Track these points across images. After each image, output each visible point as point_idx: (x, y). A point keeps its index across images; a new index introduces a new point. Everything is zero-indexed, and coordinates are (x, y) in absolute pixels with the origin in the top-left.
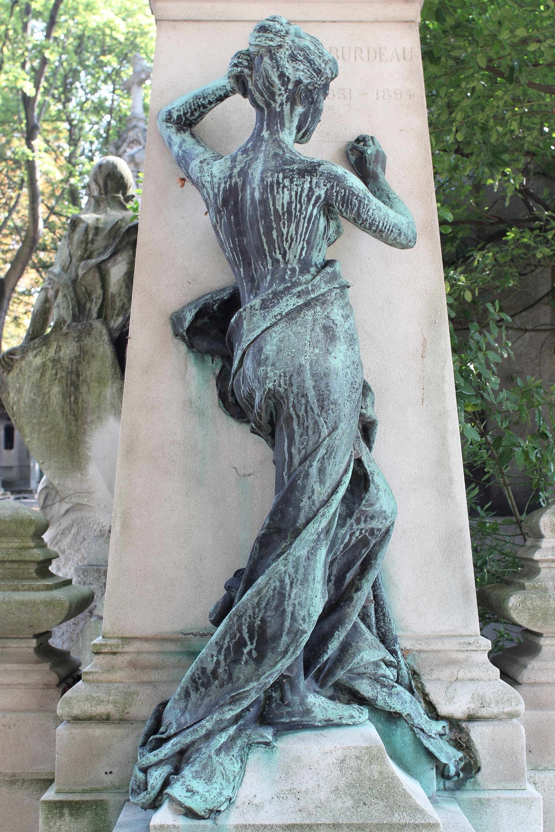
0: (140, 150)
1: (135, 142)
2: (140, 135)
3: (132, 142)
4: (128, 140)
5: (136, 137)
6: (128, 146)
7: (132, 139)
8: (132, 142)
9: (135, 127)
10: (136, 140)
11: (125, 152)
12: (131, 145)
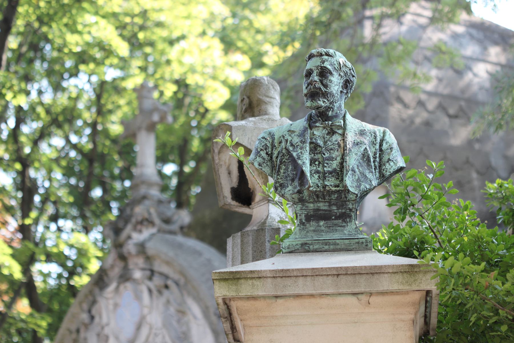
0: (153, 235)
1: (145, 223)
2: (152, 211)
3: (141, 223)
4: (134, 220)
5: (146, 215)
6: (135, 229)
7: (140, 218)
8: (141, 223)
9: (144, 197)
10: (147, 220)
11: (129, 237)
12: (139, 227)
